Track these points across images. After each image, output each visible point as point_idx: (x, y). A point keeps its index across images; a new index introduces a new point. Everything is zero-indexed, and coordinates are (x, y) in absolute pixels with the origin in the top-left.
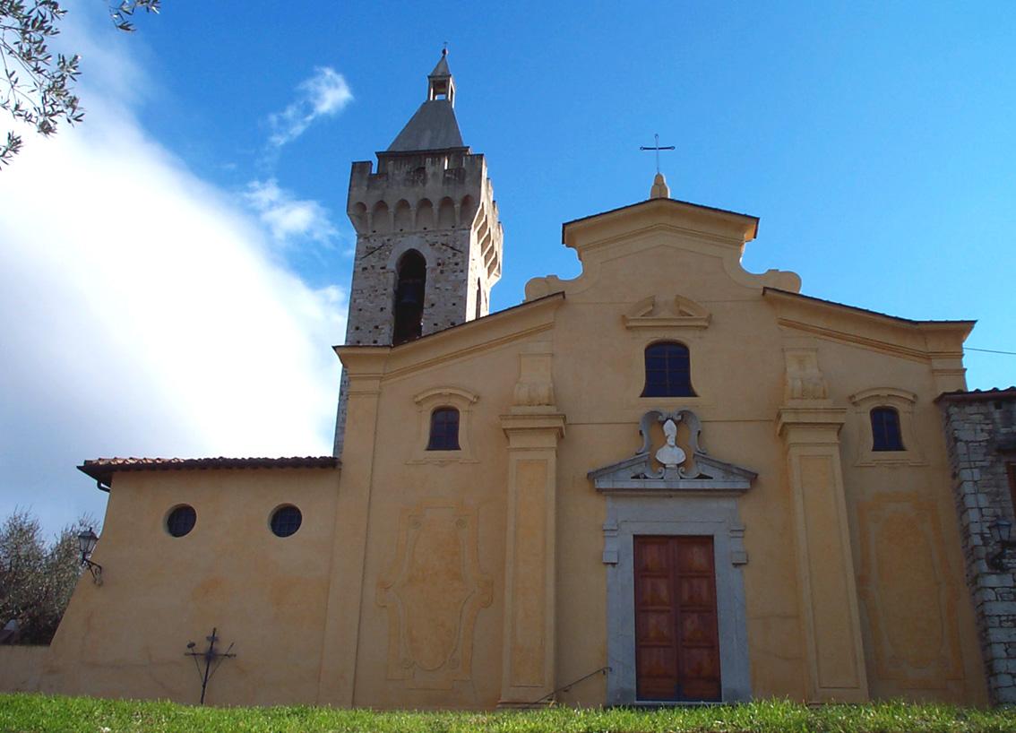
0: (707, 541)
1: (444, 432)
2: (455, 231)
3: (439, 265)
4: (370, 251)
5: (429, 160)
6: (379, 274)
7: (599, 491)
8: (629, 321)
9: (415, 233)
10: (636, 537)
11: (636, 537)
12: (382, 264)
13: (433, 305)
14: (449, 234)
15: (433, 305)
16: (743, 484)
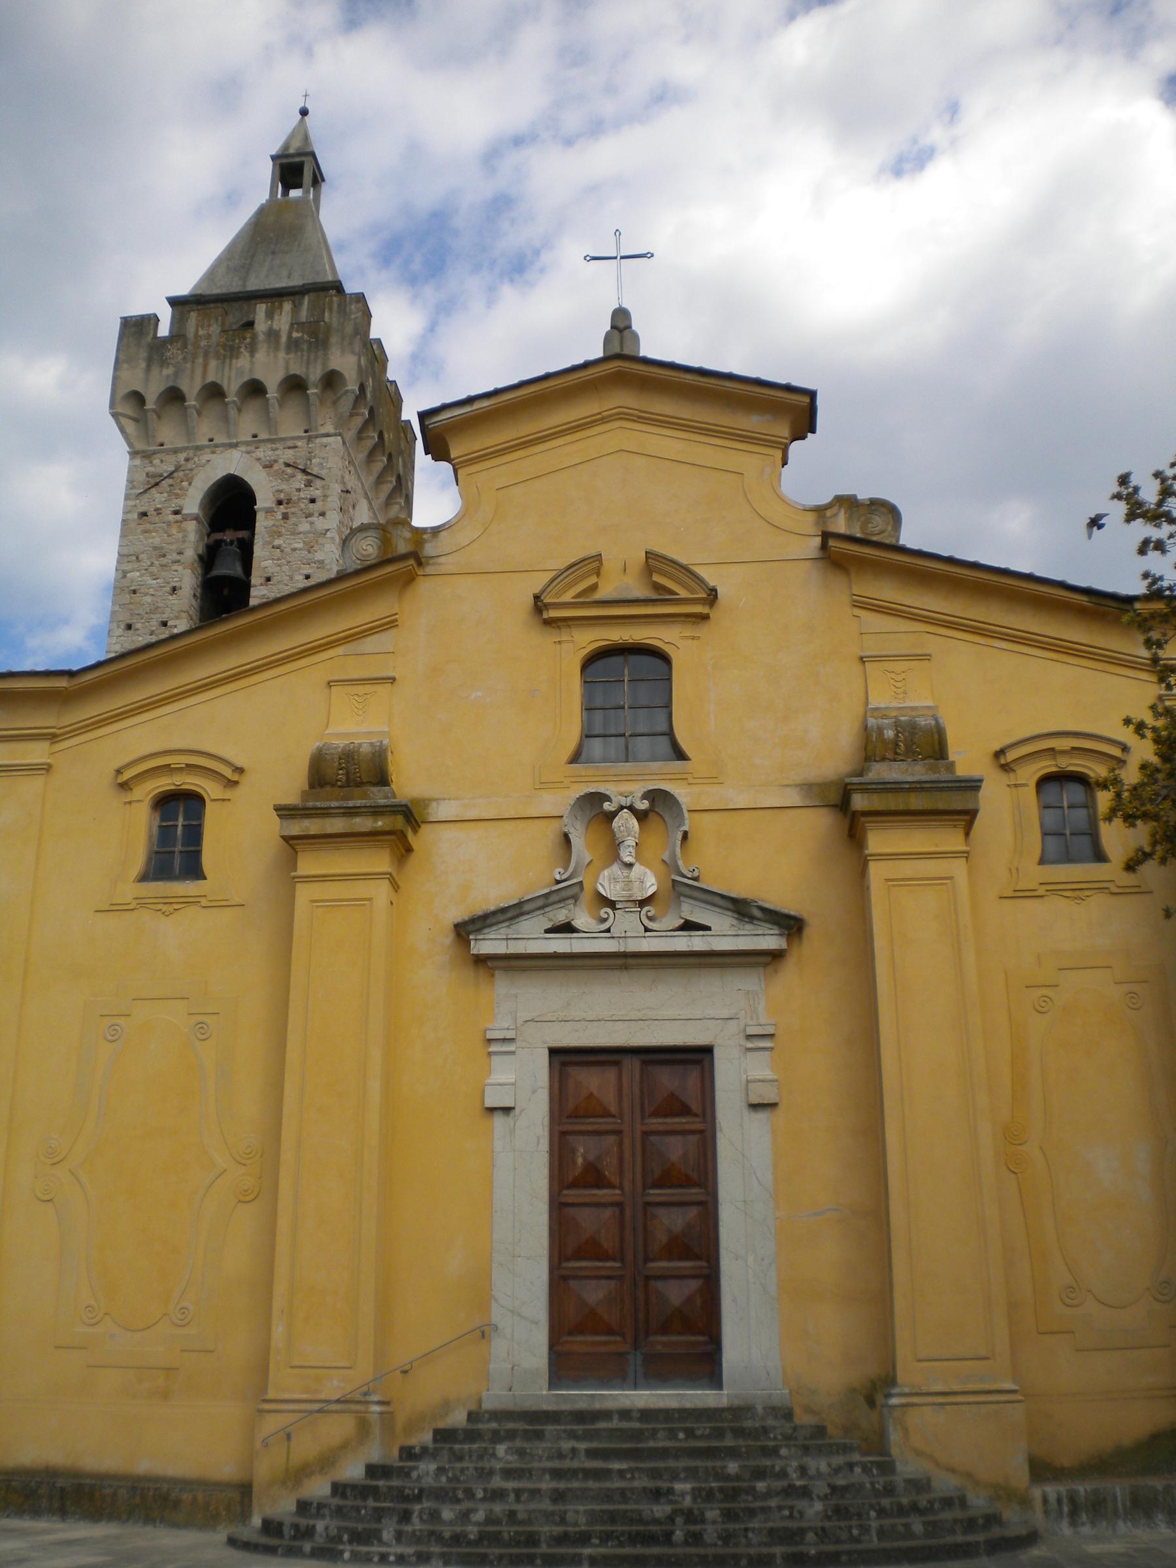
0: (699, 1057)
1: (177, 838)
2: (309, 439)
3: (280, 503)
4: (153, 481)
5: (261, 309)
6: (169, 524)
7: (481, 961)
8: (547, 606)
9: (234, 446)
10: (554, 1052)
11: (554, 1052)
13: (268, 579)
14: (299, 444)
15: (268, 579)
16: (770, 941)
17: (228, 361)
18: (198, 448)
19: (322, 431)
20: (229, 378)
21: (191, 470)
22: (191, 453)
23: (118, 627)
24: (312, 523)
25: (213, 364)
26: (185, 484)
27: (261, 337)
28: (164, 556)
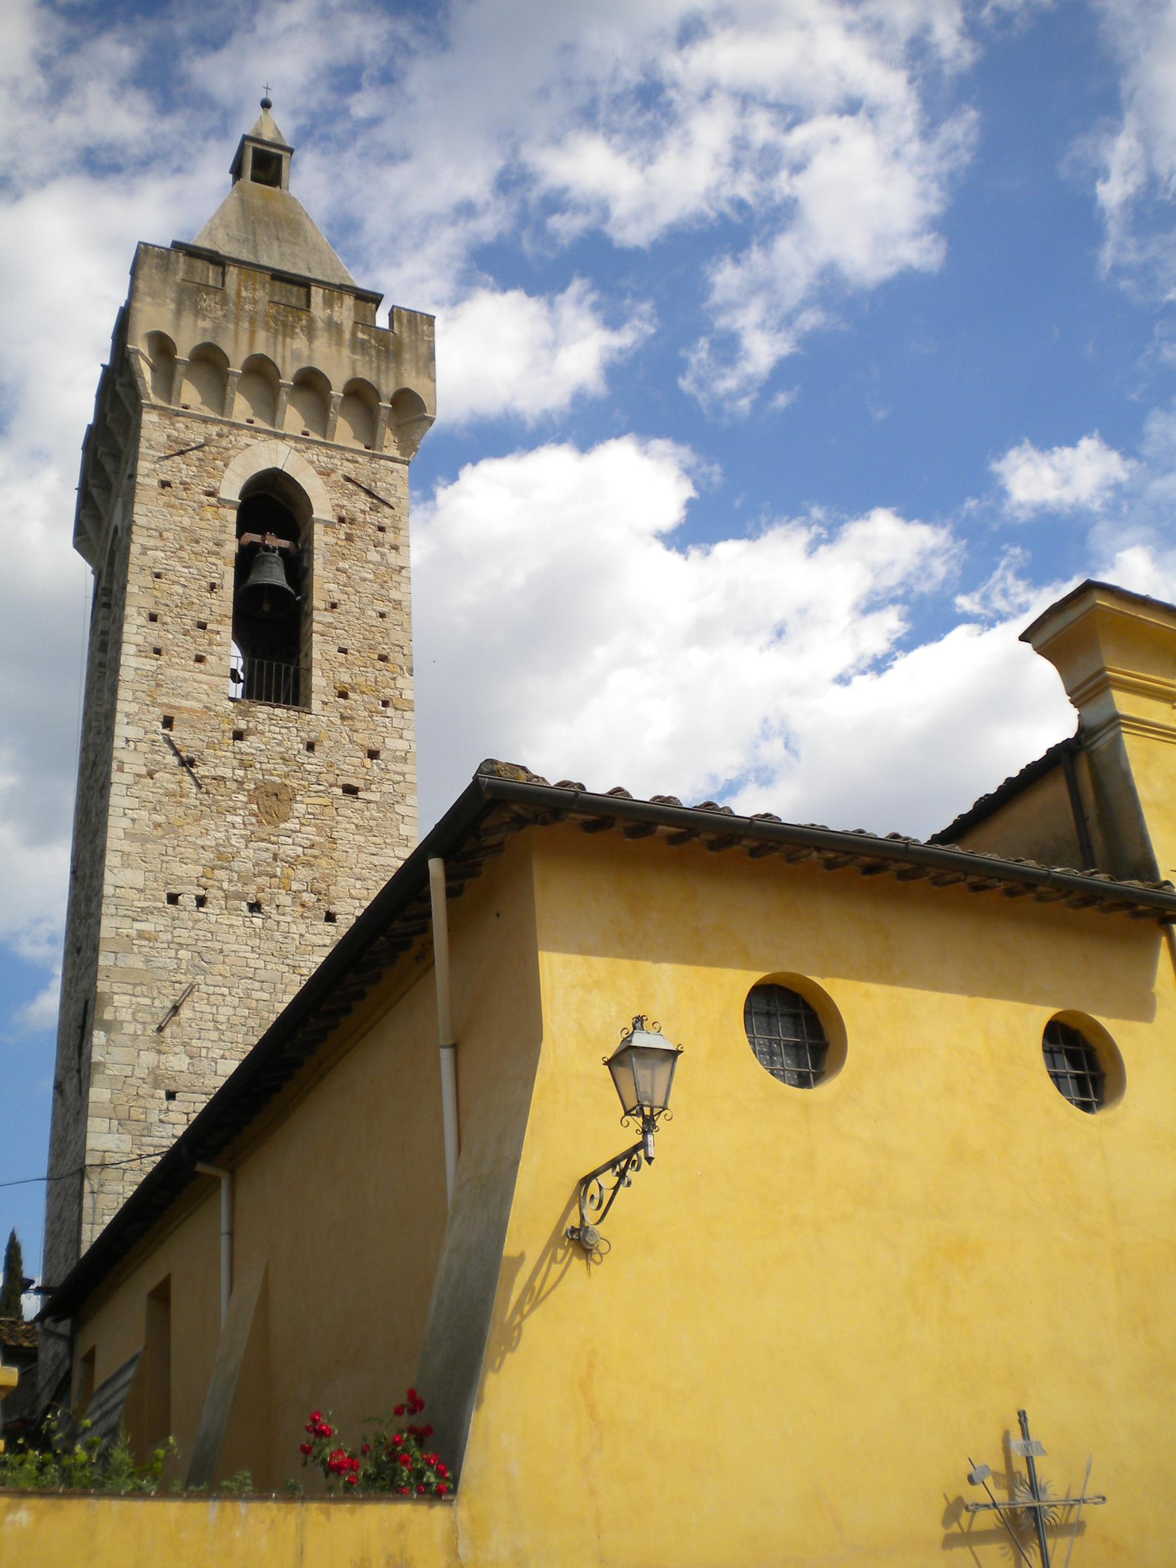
3: (342, 520)
4: (177, 448)
6: (201, 505)
9: (283, 437)
13: (334, 606)
14: (360, 459)
15: (334, 606)
17: (280, 338)
18: (234, 425)
19: (386, 452)
20: (284, 358)
21: (227, 449)
22: (226, 429)
23: (139, 614)
24: (383, 555)
25: (262, 335)
26: (220, 463)
27: (320, 324)
28: (197, 542)
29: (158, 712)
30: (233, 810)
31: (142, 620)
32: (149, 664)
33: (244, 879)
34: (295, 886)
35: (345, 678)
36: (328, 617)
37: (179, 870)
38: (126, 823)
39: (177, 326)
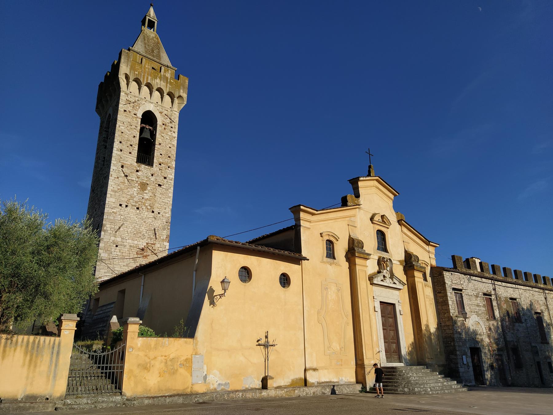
12: (135, 112)
29: (120, 164)
30: (135, 187)
31: (118, 143)
32: (119, 153)
33: (136, 202)
34: (146, 205)
35: (161, 161)
36: (159, 146)
37: (123, 199)
38: (112, 188)
39: (130, 72)
